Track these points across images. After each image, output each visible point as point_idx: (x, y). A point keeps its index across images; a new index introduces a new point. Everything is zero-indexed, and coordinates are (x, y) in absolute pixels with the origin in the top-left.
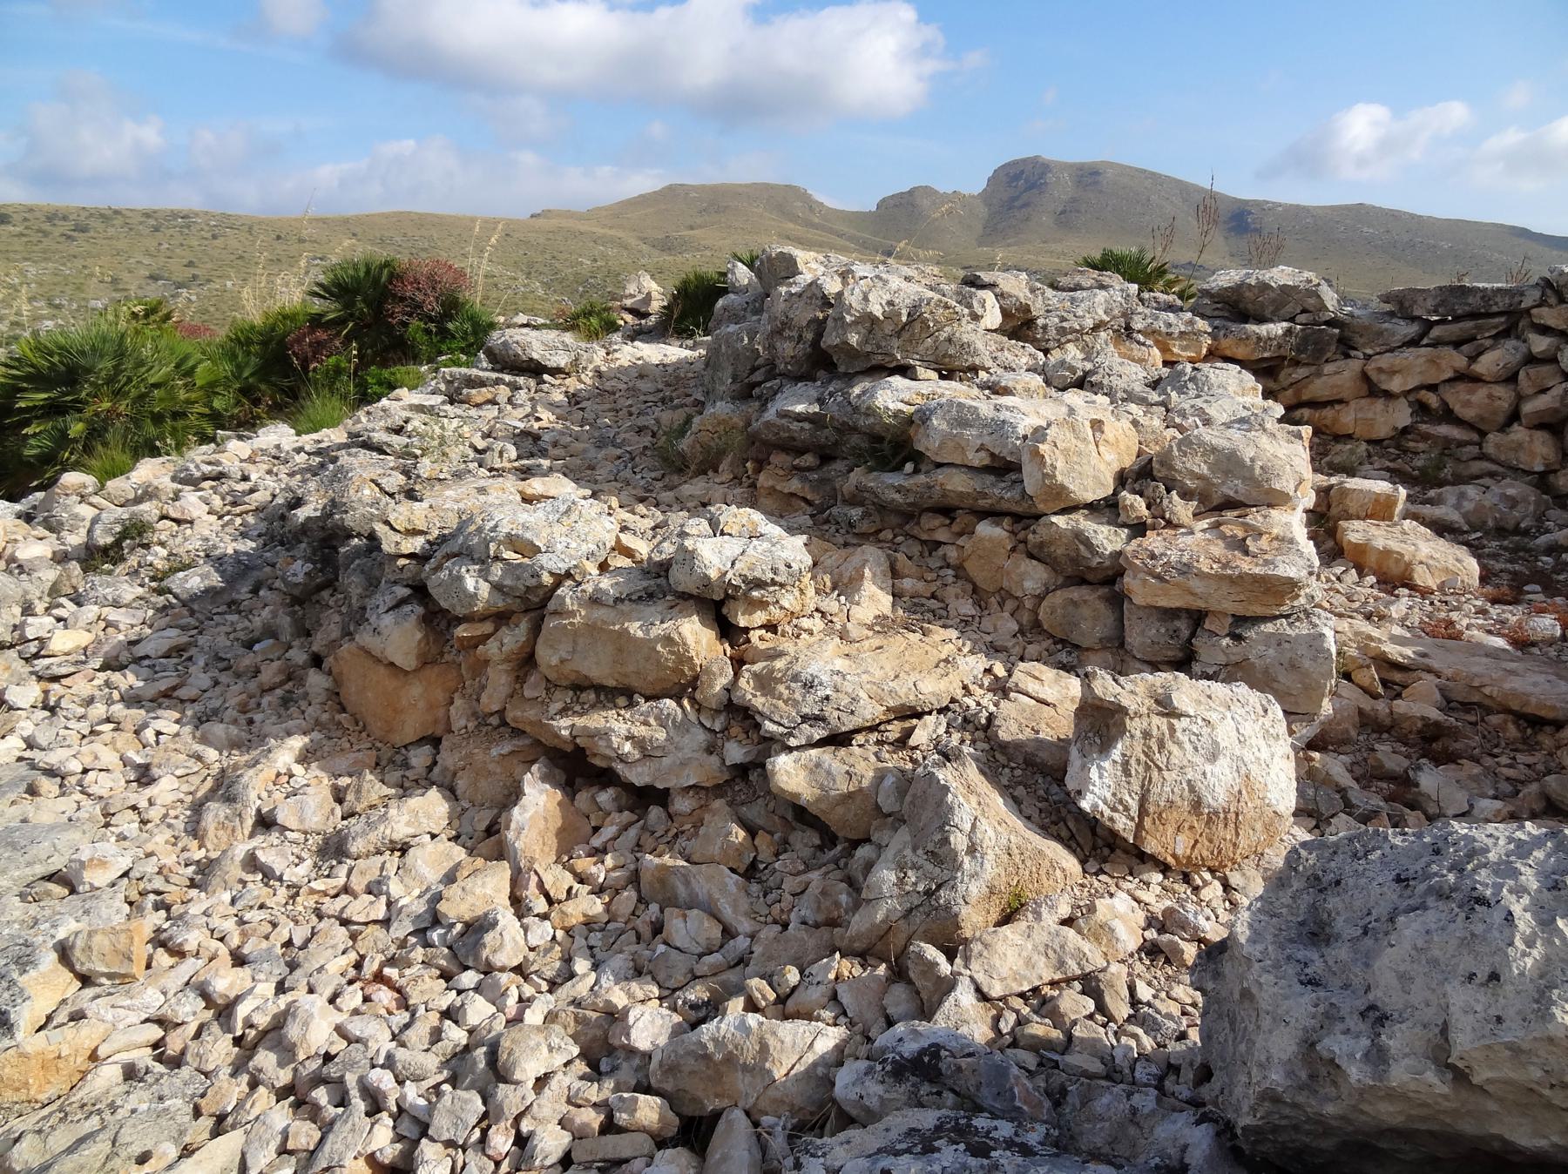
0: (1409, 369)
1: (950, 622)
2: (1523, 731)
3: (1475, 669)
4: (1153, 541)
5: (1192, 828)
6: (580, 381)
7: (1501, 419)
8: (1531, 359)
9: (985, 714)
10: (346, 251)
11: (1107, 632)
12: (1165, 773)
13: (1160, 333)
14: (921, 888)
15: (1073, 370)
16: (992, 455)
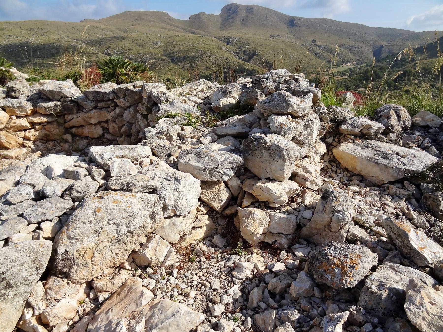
13: (11, 107)
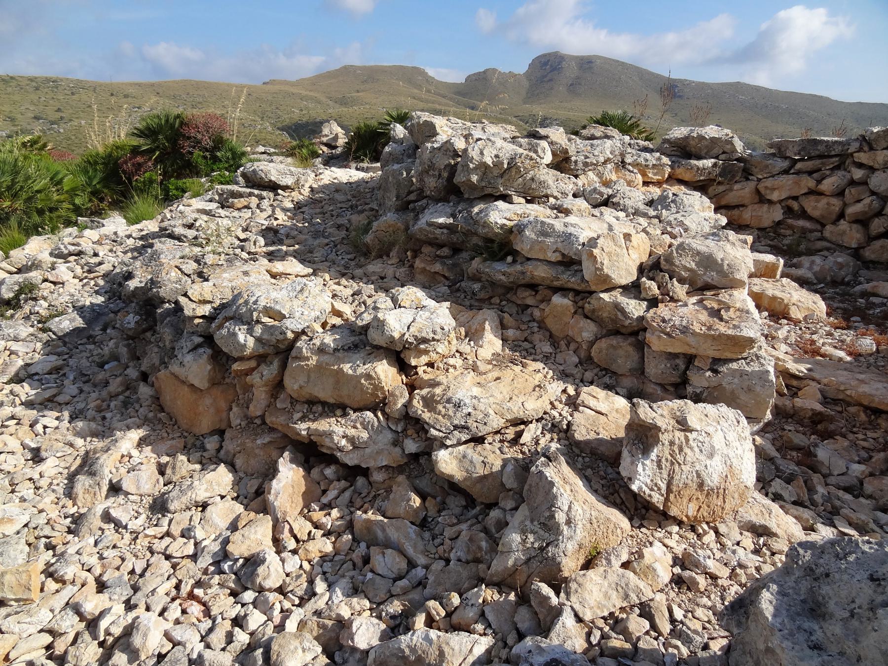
0: (782, 188)
1: (537, 357)
2: (869, 417)
3: (841, 379)
4: (663, 310)
5: (697, 499)
6: (300, 193)
7: (834, 217)
8: (852, 183)
9: (565, 422)
10: (155, 107)
11: (634, 365)
12: (683, 466)
13: (641, 165)
14: (536, 545)
15: (601, 194)
16: (563, 255)
